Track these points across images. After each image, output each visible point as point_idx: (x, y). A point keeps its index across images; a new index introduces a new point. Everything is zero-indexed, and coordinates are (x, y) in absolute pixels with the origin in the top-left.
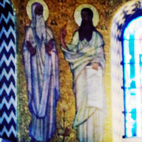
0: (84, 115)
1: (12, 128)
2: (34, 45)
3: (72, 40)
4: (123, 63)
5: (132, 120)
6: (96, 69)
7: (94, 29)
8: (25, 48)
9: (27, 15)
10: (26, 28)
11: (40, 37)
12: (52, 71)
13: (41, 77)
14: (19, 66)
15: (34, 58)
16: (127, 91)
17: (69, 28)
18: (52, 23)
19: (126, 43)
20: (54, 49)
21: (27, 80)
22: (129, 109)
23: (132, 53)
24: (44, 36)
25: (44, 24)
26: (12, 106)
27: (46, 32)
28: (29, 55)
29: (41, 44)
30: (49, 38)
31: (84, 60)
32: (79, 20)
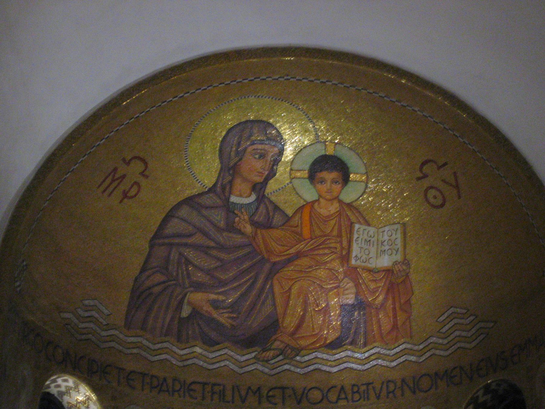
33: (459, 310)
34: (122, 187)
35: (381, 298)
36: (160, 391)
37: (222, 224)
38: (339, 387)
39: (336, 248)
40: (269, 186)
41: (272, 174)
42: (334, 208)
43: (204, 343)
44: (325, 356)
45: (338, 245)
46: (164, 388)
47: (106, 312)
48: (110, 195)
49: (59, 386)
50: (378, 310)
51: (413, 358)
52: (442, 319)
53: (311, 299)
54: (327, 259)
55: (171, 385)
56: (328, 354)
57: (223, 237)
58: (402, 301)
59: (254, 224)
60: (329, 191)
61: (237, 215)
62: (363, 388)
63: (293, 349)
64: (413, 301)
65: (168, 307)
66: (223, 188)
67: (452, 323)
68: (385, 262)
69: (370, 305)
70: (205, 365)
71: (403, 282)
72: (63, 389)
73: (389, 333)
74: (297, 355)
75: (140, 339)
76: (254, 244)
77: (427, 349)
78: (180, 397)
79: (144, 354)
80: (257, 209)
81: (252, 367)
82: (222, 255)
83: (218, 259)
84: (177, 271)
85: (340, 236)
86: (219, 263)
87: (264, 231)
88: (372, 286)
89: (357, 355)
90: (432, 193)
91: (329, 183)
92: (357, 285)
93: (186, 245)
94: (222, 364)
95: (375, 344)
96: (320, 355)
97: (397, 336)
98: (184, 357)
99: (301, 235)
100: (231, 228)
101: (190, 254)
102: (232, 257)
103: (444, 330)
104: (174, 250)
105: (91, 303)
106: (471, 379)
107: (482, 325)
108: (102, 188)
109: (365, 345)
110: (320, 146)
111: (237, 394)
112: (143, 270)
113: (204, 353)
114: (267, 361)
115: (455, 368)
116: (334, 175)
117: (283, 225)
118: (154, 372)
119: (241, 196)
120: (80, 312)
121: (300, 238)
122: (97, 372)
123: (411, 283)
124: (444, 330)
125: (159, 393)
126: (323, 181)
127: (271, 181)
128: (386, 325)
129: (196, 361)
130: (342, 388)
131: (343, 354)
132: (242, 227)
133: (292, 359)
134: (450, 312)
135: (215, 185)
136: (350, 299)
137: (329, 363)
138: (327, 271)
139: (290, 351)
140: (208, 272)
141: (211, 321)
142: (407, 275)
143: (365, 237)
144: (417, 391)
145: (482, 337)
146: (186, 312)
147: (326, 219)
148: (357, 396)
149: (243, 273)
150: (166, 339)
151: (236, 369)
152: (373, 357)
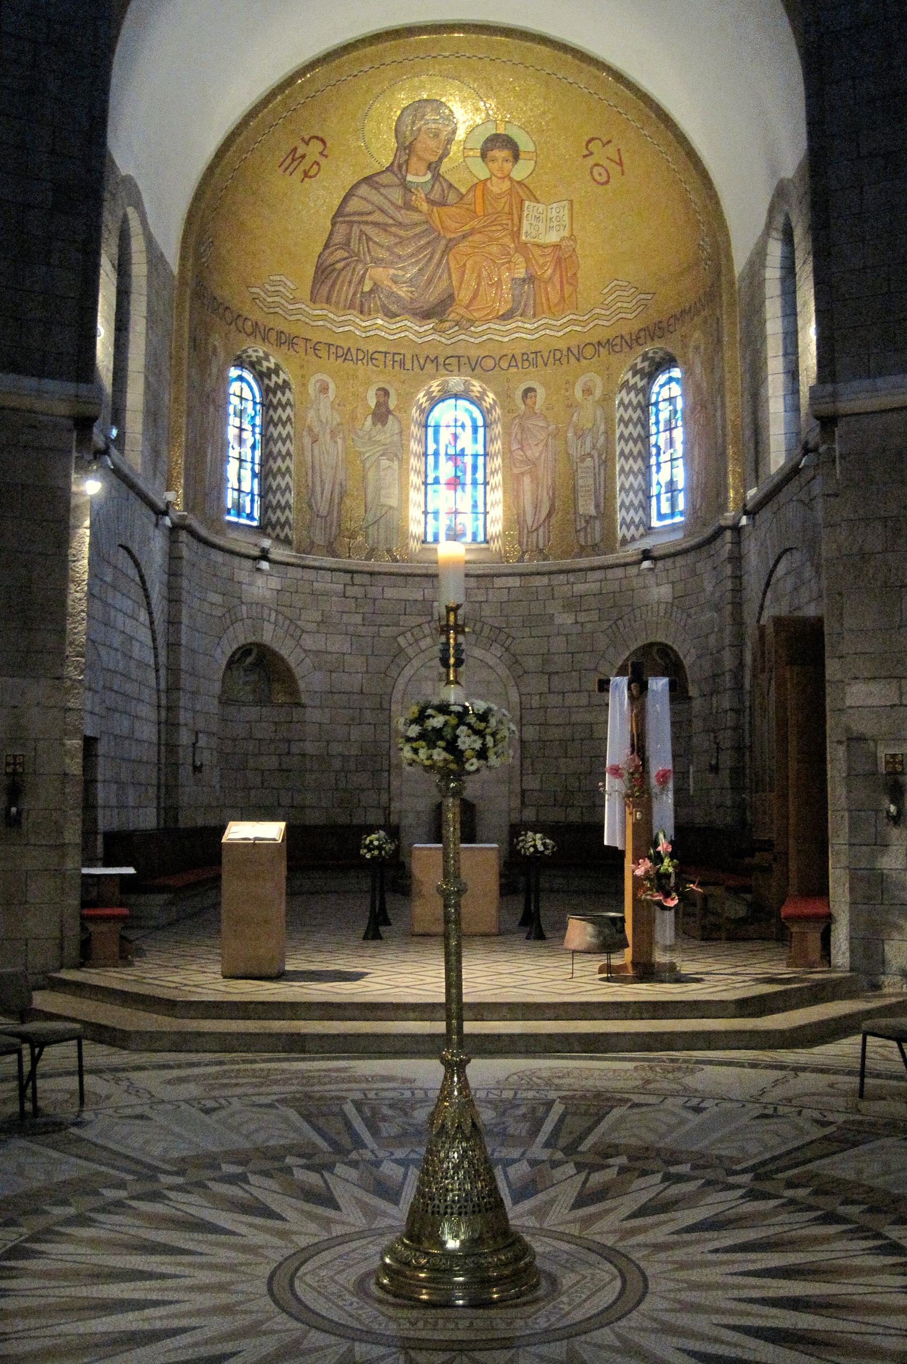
0: (375, 515)
1: (287, 529)
2: (316, 430)
4: (425, 454)
6: (392, 460)
7: (389, 412)
8: (305, 433)
13: (324, 470)
15: (315, 446)
17: (360, 410)
19: (430, 431)
22: (429, 510)
23: (436, 441)
26: (287, 502)
30: (335, 423)
32: (372, 403)
34: (302, 168)
35: (550, 271)
37: (400, 202)
40: (443, 165)
41: (445, 154)
42: (506, 185)
44: (497, 327)
46: (349, 357)
49: (250, 356)
50: (546, 283)
52: (605, 291)
53: (485, 274)
60: (501, 169)
63: (469, 320)
65: (350, 282)
66: (400, 167)
67: (615, 295)
68: (553, 238)
70: (386, 336)
71: (570, 256)
72: (254, 359)
73: (556, 305)
75: (325, 312)
79: (329, 326)
81: (431, 338)
82: (402, 233)
83: (395, 235)
86: (398, 240)
90: (596, 170)
92: (527, 260)
93: (366, 223)
100: (408, 206)
101: (370, 230)
102: (410, 233)
104: (355, 227)
105: (278, 278)
106: (631, 348)
107: (643, 296)
108: (283, 167)
109: (534, 315)
110: (490, 126)
111: (416, 362)
112: (326, 246)
118: (339, 343)
119: (417, 175)
120: (267, 286)
121: (474, 214)
127: (445, 160)
128: (554, 298)
129: (379, 332)
131: (514, 325)
135: (392, 164)
136: (521, 273)
140: (389, 249)
143: (535, 213)
147: (498, 197)
148: (526, 364)
149: (421, 249)
150: (350, 311)
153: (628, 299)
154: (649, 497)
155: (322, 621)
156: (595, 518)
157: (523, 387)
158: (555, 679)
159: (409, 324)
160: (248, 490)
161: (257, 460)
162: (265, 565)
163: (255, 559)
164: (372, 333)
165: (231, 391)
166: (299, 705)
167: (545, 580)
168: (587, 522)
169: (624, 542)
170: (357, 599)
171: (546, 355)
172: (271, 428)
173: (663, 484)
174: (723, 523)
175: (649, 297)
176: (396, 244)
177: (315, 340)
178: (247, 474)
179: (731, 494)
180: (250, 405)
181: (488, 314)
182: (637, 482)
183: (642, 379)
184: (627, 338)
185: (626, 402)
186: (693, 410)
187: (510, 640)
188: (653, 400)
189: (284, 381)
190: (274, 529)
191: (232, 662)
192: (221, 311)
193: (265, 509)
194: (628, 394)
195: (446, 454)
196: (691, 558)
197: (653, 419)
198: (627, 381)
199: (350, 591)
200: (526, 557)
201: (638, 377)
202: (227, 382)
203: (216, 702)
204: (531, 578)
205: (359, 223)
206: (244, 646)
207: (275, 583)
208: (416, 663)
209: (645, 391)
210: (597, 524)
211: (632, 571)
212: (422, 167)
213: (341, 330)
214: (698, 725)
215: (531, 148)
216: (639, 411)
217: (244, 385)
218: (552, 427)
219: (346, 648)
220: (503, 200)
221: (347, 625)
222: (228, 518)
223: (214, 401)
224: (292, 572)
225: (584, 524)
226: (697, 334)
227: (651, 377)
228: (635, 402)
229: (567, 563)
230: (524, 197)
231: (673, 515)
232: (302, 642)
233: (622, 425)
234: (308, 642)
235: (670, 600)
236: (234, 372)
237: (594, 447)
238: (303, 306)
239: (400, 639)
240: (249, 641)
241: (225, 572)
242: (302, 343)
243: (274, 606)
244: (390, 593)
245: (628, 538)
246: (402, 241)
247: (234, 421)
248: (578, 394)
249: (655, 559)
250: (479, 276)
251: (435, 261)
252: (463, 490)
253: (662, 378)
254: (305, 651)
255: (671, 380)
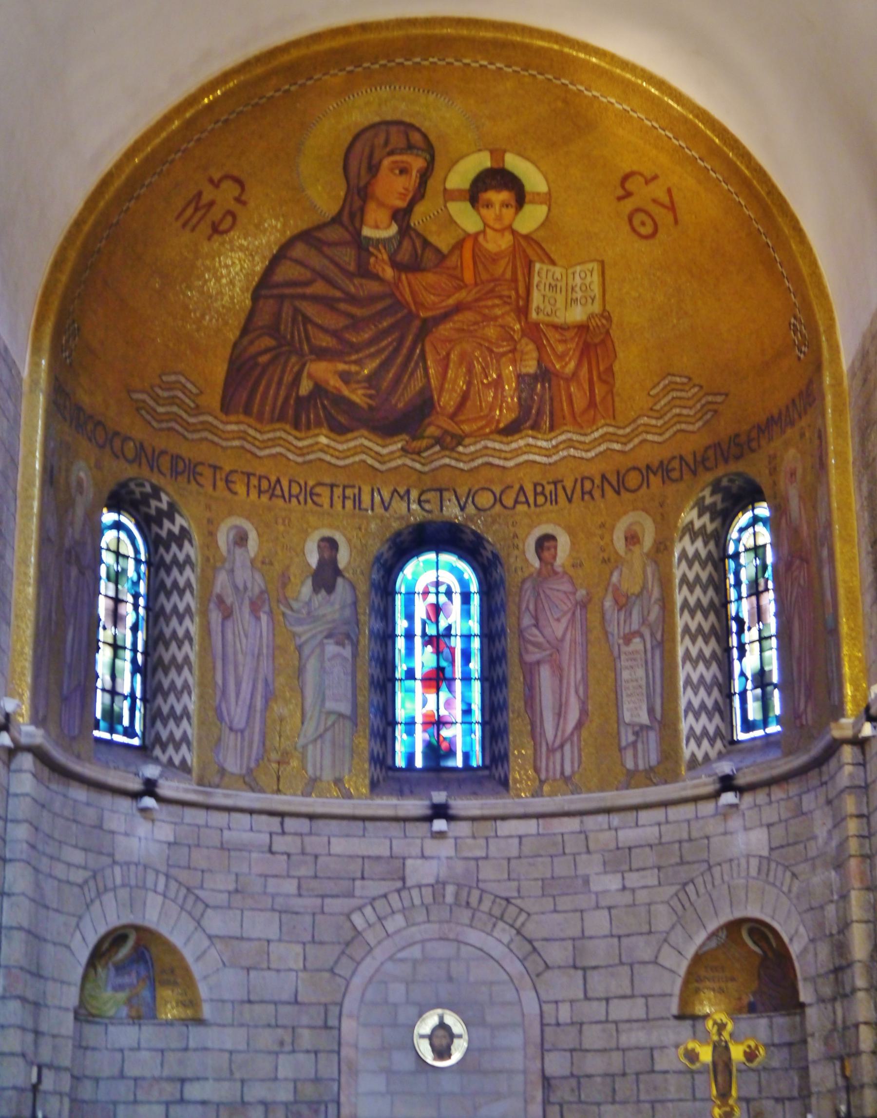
0: (317, 728)
2: (229, 601)
3: (299, 592)
5: (405, 736)
6: (343, 645)
7: (337, 572)
9: (218, 547)
10: (215, 569)
11: (241, 587)
12: (260, 649)
13: (240, 657)
14: (202, 638)
15: (229, 624)
16: (397, 684)
17: (294, 570)
18: (263, 563)
19: (399, 601)
20: (266, 608)
21: (214, 663)
23: (410, 617)
24: (249, 585)
25: (249, 564)
26: (185, 708)
27: (253, 577)
28: (220, 620)
29: (243, 600)
30: (257, 590)
31: (319, 629)
32: (313, 560)
33: (678, 379)
35: (572, 365)
36: (272, 496)
37: (352, 268)
38: (517, 487)
39: (510, 297)
41: (419, 194)
42: (505, 242)
43: (332, 429)
44: (497, 446)
45: (513, 293)
46: (278, 492)
47: (194, 390)
48: (193, 229)
49: (132, 492)
50: (568, 380)
51: (617, 446)
53: (478, 368)
54: (498, 312)
55: (286, 489)
56: (501, 442)
57: (354, 285)
58: (602, 368)
59: (395, 265)
60: (499, 218)
61: (371, 254)
62: (549, 488)
63: (453, 436)
64: (616, 368)
65: (280, 383)
66: (352, 216)
67: (669, 397)
68: (577, 315)
69: (557, 375)
70: (334, 461)
71: (603, 342)
72: (138, 496)
73: (585, 412)
74: (459, 444)
75: (242, 427)
76: (398, 294)
77: (636, 432)
78: (299, 502)
79: (248, 446)
80: (400, 243)
81: (399, 462)
84: (292, 334)
85: (515, 280)
87: (410, 276)
88: (560, 348)
89: (540, 443)
91: (497, 207)
92: (540, 348)
93: (304, 297)
94: (357, 458)
95: (565, 428)
96: (490, 444)
97: (595, 416)
98: (305, 451)
99: (462, 280)
100: (365, 272)
101: (310, 309)
103: (658, 407)
105: (173, 378)
106: (694, 473)
107: (710, 398)
109: (552, 428)
111: (377, 498)
112: (245, 331)
113: (333, 444)
114: (419, 453)
115: (674, 458)
116: (504, 196)
117: (436, 266)
119: (377, 227)
122: (184, 472)
123: (612, 341)
124: (658, 407)
125: (270, 498)
126: (489, 205)
128: (580, 403)
130: (522, 488)
131: (522, 443)
132: (380, 269)
133: (453, 449)
134: (666, 382)
136: (530, 367)
137: (503, 455)
138: (499, 329)
139: (448, 439)
140: (335, 334)
141: (340, 400)
142: (608, 333)
143: (550, 280)
144: (622, 491)
145: (709, 416)
146: (305, 387)
147: (494, 259)
148: (540, 499)
150: (278, 426)
151: (377, 465)
152: (561, 446)
153: (691, 403)
154: (730, 696)
155: (237, 891)
156: (648, 728)
157: (537, 532)
158: (594, 978)
159: (366, 443)
160: (126, 691)
161: (140, 647)
162: (149, 802)
163: (136, 796)
164: (311, 457)
165: (103, 545)
166: (199, 1022)
167: (572, 824)
168: (636, 734)
169: (693, 763)
170: (289, 855)
171: (569, 485)
172: (162, 598)
173: (749, 675)
174: (837, 733)
175: (719, 399)
176: (346, 328)
177: (227, 468)
178: (125, 666)
179: (849, 690)
180: (131, 564)
181: (482, 428)
182: (710, 673)
183: (712, 520)
184: (690, 459)
185: (690, 552)
186: (789, 566)
187: (523, 916)
188: (731, 550)
189: (182, 529)
190: (164, 749)
191: (98, 955)
192: (90, 427)
193: (150, 719)
194: (693, 541)
195: (424, 634)
196: (793, 788)
197: (731, 579)
198: (691, 523)
199: (280, 844)
200: (546, 788)
201: (706, 518)
202: (99, 532)
203: (71, 1016)
204: (555, 821)
205: (293, 297)
206: (115, 930)
207: (165, 832)
208: (379, 954)
209: (720, 538)
210: (652, 736)
211: (707, 808)
212: (383, 216)
213: (267, 452)
214: (815, 1048)
215: (543, 188)
216: (710, 568)
217: (123, 535)
218: (581, 593)
219: (273, 932)
220: (503, 263)
221: (274, 896)
222: (96, 733)
223: (78, 558)
224: (192, 816)
225: (631, 738)
226: (792, 452)
227: (726, 518)
228: (703, 554)
229: (611, 798)
230: (533, 257)
231: (765, 723)
232: (205, 923)
233: (685, 588)
234: (215, 923)
235: (765, 853)
236: (108, 517)
237: (644, 621)
238: (210, 419)
239: (357, 919)
240: (124, 921)
241: (90, 815)
242: (208, 472)
243: (164, 868)
244: (339, 846)
245: (700, 756)
246: (356, 324)
247: (106, 588)
248: (620, 544)
249: (740, 790)
250: (470, 371)
251: (404, 351)
252: (451, 690)
253: (744, 519)
254: (210, 937)
255: (755, 520)
